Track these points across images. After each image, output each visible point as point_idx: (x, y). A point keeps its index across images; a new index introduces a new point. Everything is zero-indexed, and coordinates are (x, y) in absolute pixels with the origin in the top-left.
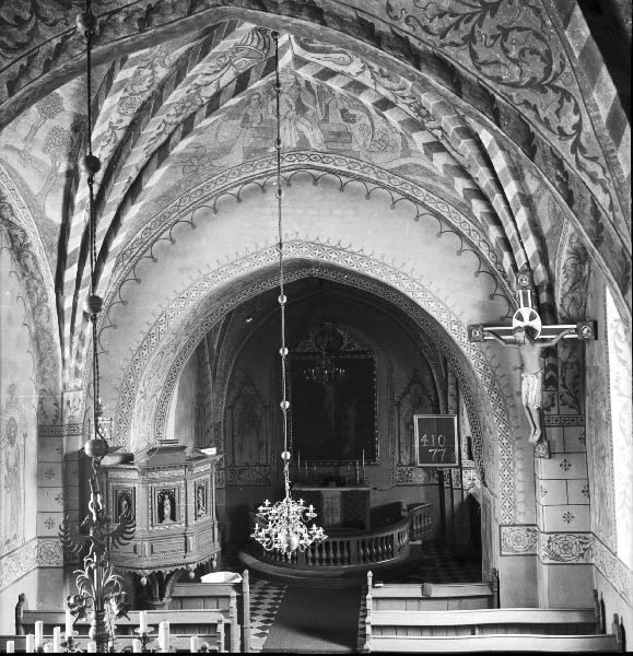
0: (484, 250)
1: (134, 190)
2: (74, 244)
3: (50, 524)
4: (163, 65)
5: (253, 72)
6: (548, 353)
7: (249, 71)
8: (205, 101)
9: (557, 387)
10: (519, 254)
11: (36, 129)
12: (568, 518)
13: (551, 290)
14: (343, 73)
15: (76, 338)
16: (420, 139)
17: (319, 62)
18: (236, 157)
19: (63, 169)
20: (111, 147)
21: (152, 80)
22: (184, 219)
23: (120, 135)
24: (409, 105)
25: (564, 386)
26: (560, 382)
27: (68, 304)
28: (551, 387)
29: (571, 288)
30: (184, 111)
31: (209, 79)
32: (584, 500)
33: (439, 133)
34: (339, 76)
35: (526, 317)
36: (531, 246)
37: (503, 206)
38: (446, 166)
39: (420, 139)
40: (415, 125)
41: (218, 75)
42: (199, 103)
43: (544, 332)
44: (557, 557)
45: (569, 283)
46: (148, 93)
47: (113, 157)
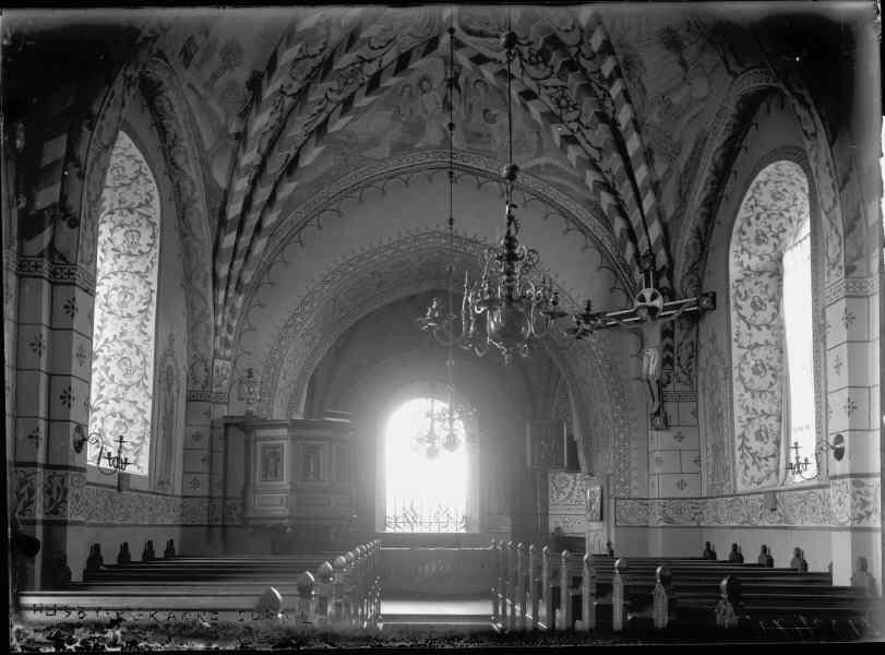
0: (607, 244)
1: (291, 167)
2: (234, 210)
3: (196, 484)
5: (414, 53)
6: (667, 333)
7: (412, 49)
8: (367, 79)
9: (672, 365)
10: (642, 241)
12: (681, 485)
13: (670, 276)
14: (494, 60)
15: (228, 309)
16: (557, 131)
17: (476, 47)
18: (384, 151)
22: (332, 207)
23: (288, 101)
24: (551, 97)
25: (679, 365)
26: (676, 361)
27: (223, 271)
28: (668, 366)
29: (690, 268)
31: (374, 54)
32: (695, 467)
33: (574, 126)
34: (491, 64)
35: (647, 293)
36: (655, 231)
37: (631, 194)
38: (579, 158)
39: (557, 131)
40: (551, 117)
41: (381, 52)
42: (361, 81)
43: (666, 309)
44: (669, 520)
45: (689, 265)
46: (319, 58)
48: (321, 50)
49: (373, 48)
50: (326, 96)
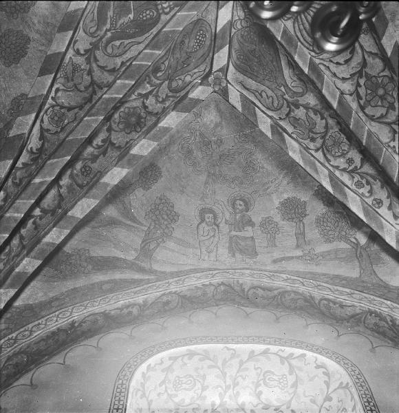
4: (302, 95)
8: (387, 73)
11: (303, 234)
19: (363, 240)
20: (377, 185)
21: (316, 112)
30: (389, 99)
31: (357, 59)
42: (386, 80)
46: (331, 121)
47: (392, 189)
48: (322, 118)
49: (347, 62)
50: (389, 124)
